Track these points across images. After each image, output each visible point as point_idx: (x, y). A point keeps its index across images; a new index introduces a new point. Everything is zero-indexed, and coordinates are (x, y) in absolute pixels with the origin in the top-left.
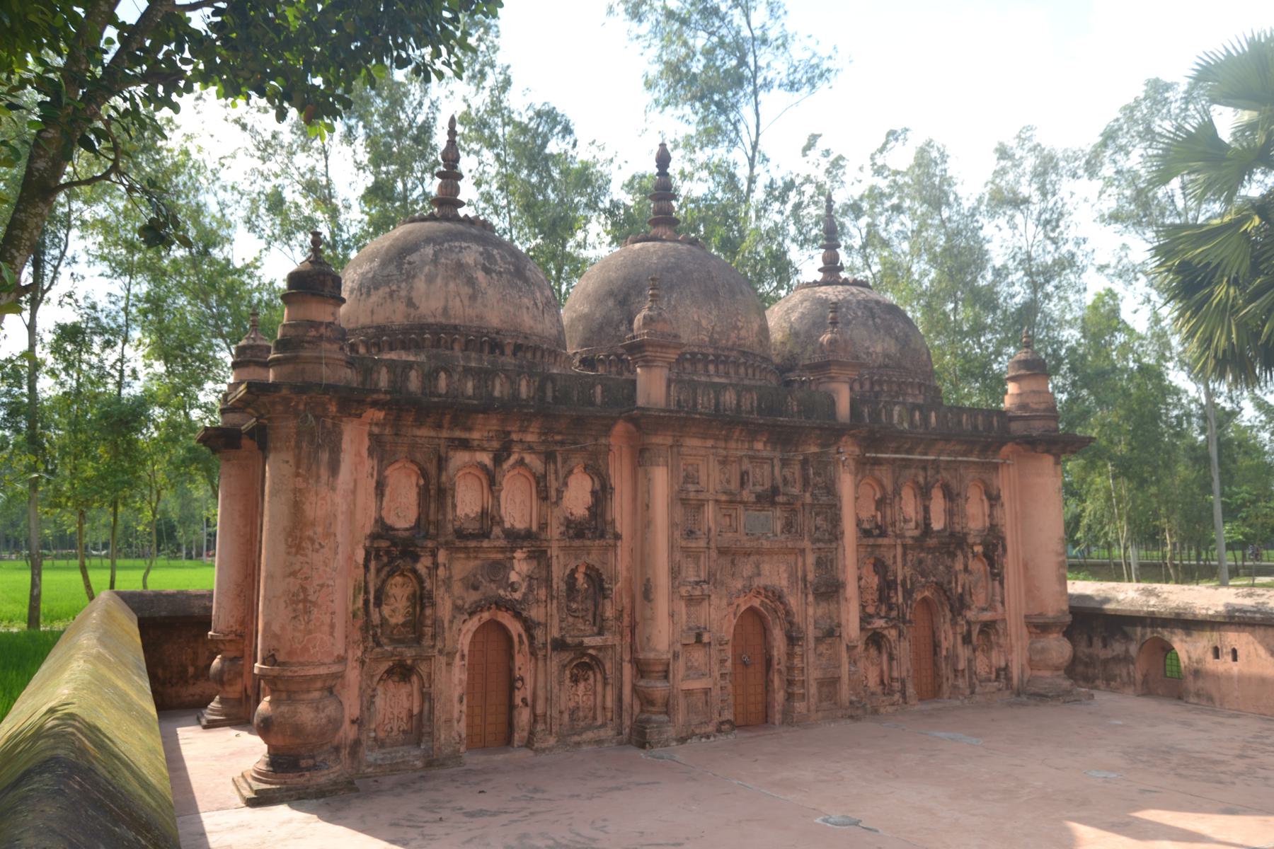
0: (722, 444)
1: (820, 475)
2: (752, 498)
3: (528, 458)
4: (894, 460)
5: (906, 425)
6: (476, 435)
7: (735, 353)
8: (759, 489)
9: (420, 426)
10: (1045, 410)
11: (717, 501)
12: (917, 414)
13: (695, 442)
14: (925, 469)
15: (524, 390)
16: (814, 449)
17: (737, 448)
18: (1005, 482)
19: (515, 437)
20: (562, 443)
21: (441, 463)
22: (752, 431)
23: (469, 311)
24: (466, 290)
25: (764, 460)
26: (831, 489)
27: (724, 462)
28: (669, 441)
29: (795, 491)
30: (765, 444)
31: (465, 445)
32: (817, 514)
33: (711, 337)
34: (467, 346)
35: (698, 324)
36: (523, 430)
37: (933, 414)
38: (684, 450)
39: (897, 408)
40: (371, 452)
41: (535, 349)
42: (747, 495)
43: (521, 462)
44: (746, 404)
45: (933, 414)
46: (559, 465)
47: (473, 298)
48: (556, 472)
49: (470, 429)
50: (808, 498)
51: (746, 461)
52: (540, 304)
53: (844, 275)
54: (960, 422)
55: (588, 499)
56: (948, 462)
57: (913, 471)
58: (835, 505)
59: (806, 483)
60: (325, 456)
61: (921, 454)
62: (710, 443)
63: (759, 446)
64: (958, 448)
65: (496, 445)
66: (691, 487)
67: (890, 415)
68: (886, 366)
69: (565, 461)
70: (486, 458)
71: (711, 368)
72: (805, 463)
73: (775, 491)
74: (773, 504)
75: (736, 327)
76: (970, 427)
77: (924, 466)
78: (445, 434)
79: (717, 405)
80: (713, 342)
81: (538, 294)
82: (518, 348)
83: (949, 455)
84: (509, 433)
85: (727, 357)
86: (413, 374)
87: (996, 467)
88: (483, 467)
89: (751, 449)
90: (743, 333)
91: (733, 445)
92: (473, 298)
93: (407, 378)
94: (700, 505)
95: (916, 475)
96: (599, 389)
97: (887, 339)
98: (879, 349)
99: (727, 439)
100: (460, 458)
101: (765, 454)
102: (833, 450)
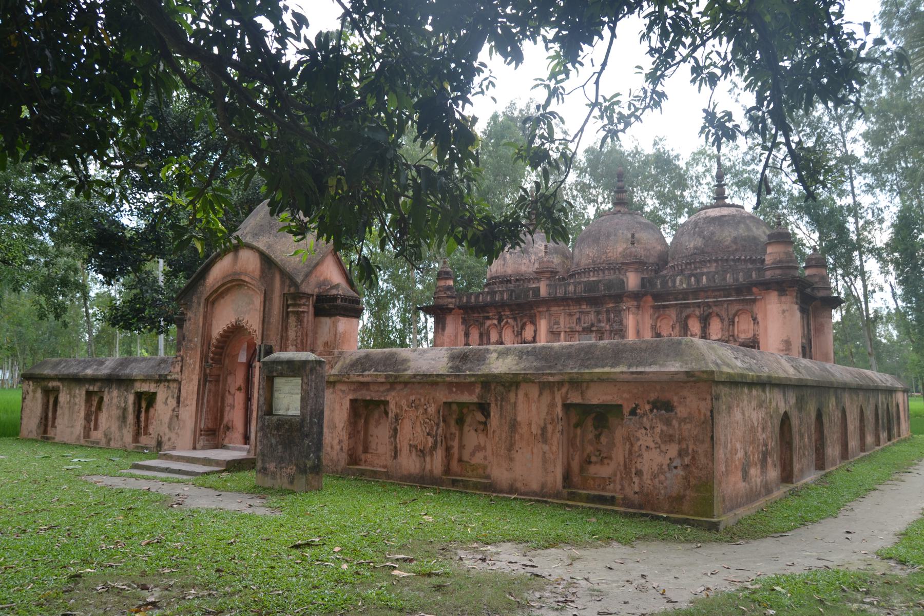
0: (567, 308)
1: (617, 316)
2: (581, 329)
3: (509, 321)
4: (676, 304)
5: (684, 286)
6: (491, 314)
7: (604, 265)
8: (586, 325)
9: (474, 313)
10: (772, 264)
11: (565, 332)
12: (693, 279)
13: (556, 308)
14: (699, 307)
15: (505, 297)
16: (611, 305)
17: (574, 309)
18: (757, 308)
19: (502, 313)
20: (518, 314)
21: (482, 324)
22: (578, 301)
23: (503, 270)
24: (503, 262)
25: (588, 313)
26: (621, 323)
27: (570, 315)
28: (545, 309)
29: (603, 325)
30: (587, 305)
31: (488, 318)
32: (615, 334)
33: (593, 260)
34: (501, 282)
35: (588, 255)
36: (504, 311)
37: (704, 277)
38: (552, 312)
39: (679, 278)
40: (462, 323)
41: (524, 280)
42: (578, 328)
43: (507, 322)
44: (579, 289)
45: (704, 277)
46: (519, 322)
47: (504, 265)
48: (517, 325)
49: (488, 313)
50: (608, 327)
51: (578, 314)
52: (533, 261)
53: (728, 201)
54: (725, 279)
55: (533, 333)
56: (714, 302)
57: (692, 309)
58: (622, 330)
59: (608, 320)
60: (440, 326)
61: (693, 299)
62: (562, 308)
63: (584, 307)
64: (717, 293)
65: (497, 317)
66: (556, 326)
67: (674, 282)
68: (695, 254)
69: (521, 321)
70: (496, 322)
71: (591, 274)
72: (608, 312)
73: (592, 325)
74: (592, 331)
75: (606, 253)
76: (732, 281)
77: (698, 305)
78: (482, 315)
79: (565, 292)
80: (594, 262)
81: (533, 257)
82: (517, 280)
83: (714, 298)
84: (500, 312)
85: (599, 268)
86: (473, 297)
87: (754, 301)
88: (495, 325)
89: (580, 308)
90: (609, 255)
91: (572, 308)
92: (504, 265)
93: (471, 298)
94: (559, 333)
95: (694, 311)
96: (531, 292)
97: (698, 239)
98: (692, 245)
99: (569, 306)
100: (488, 323)
101: (588, 310)
102: (621, 305)
